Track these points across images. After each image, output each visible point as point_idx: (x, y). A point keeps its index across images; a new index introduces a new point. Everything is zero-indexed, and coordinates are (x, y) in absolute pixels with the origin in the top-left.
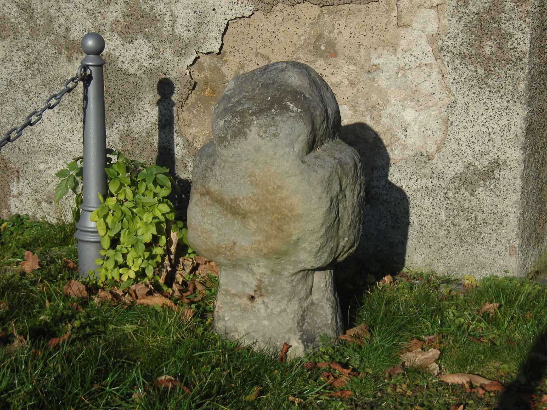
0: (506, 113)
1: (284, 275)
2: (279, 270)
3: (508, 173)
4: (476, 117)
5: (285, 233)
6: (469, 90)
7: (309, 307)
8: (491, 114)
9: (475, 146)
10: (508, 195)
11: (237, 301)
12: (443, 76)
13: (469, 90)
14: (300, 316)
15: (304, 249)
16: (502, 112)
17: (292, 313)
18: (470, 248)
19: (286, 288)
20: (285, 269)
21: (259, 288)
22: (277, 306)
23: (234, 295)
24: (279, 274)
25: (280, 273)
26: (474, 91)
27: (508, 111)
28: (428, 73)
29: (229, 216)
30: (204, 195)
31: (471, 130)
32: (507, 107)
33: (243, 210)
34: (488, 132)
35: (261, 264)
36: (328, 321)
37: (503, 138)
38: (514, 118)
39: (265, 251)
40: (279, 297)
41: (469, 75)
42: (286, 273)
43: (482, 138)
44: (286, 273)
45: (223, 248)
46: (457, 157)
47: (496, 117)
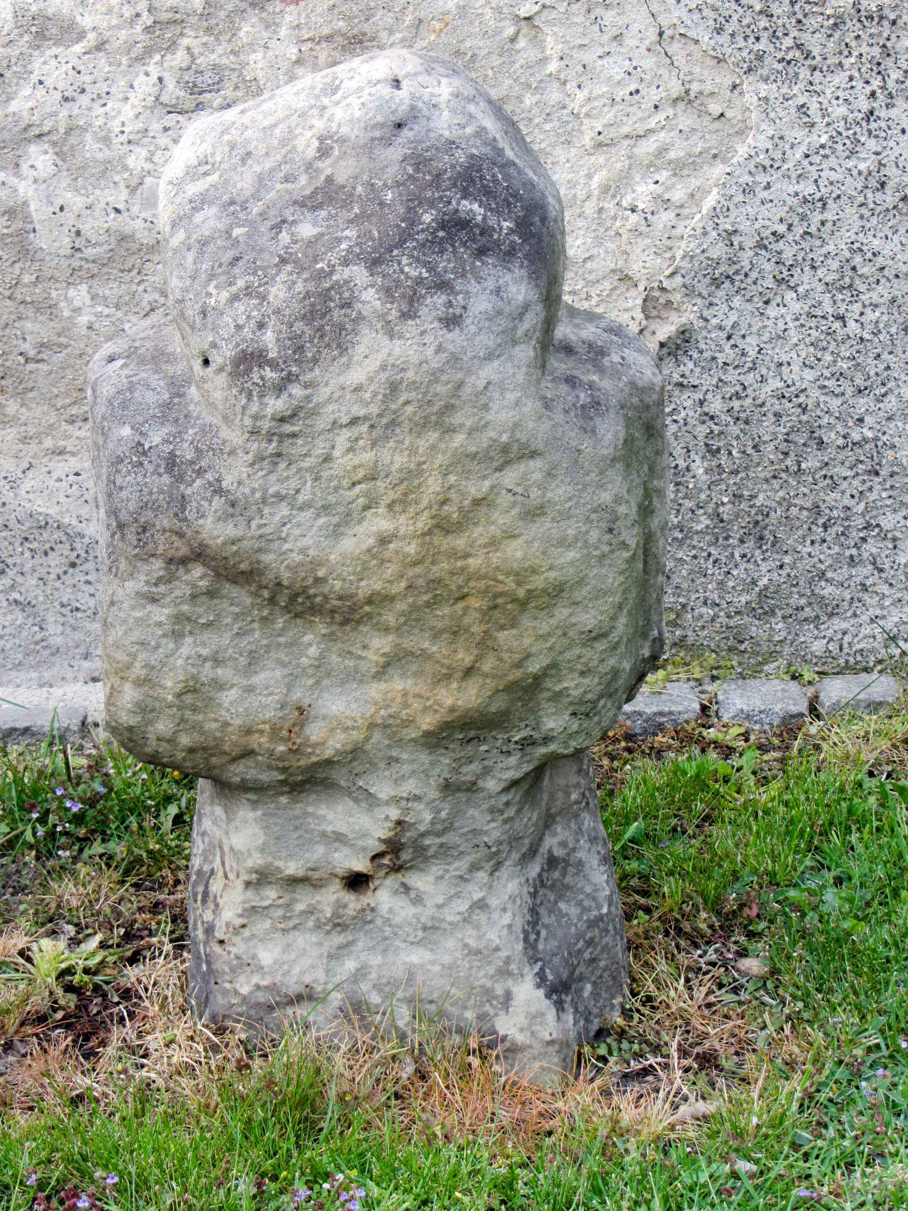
0: (870, 132)
1: (482, 790)
2: (468, 778)
3: (885, 318)
4: (778, 155)
5: (506, 656)
6: (750, 70)
7: (545, 875)
8: (823, 140)
9: (781, 245)
10: (891, 385)
11: (304, 900)
12: (661, 34)
13: (750, 70)
14: (526, 911)
15: (557, 696)
16: (858, 129)
17: (504, 910)
18: (787, 559)
19: (486, 833)
20: (487, 771)
21: (393, 846)
22: (457, 895)
23: (294, 882)
24: (468, 790)
25: (472, 788)
26: (765, 72)
27: (873, 126)
28: (615, 32)
29: (280, 623)
30: (184, 561)
31: (765, 194)
32: (872, 113)
33: (340, 598)
34: (818, 196)
35: (406, 768)
36: (599, 907)
37: (863, 211)
38: (892, 144)
39: (427, 722)
40: (462, 865)
41: (745, 22)
42: (492, 785)
43: (803, 218)
44: (492, 785)
45: (261, 732)
46: (727, 284)
47: (840, 147)
